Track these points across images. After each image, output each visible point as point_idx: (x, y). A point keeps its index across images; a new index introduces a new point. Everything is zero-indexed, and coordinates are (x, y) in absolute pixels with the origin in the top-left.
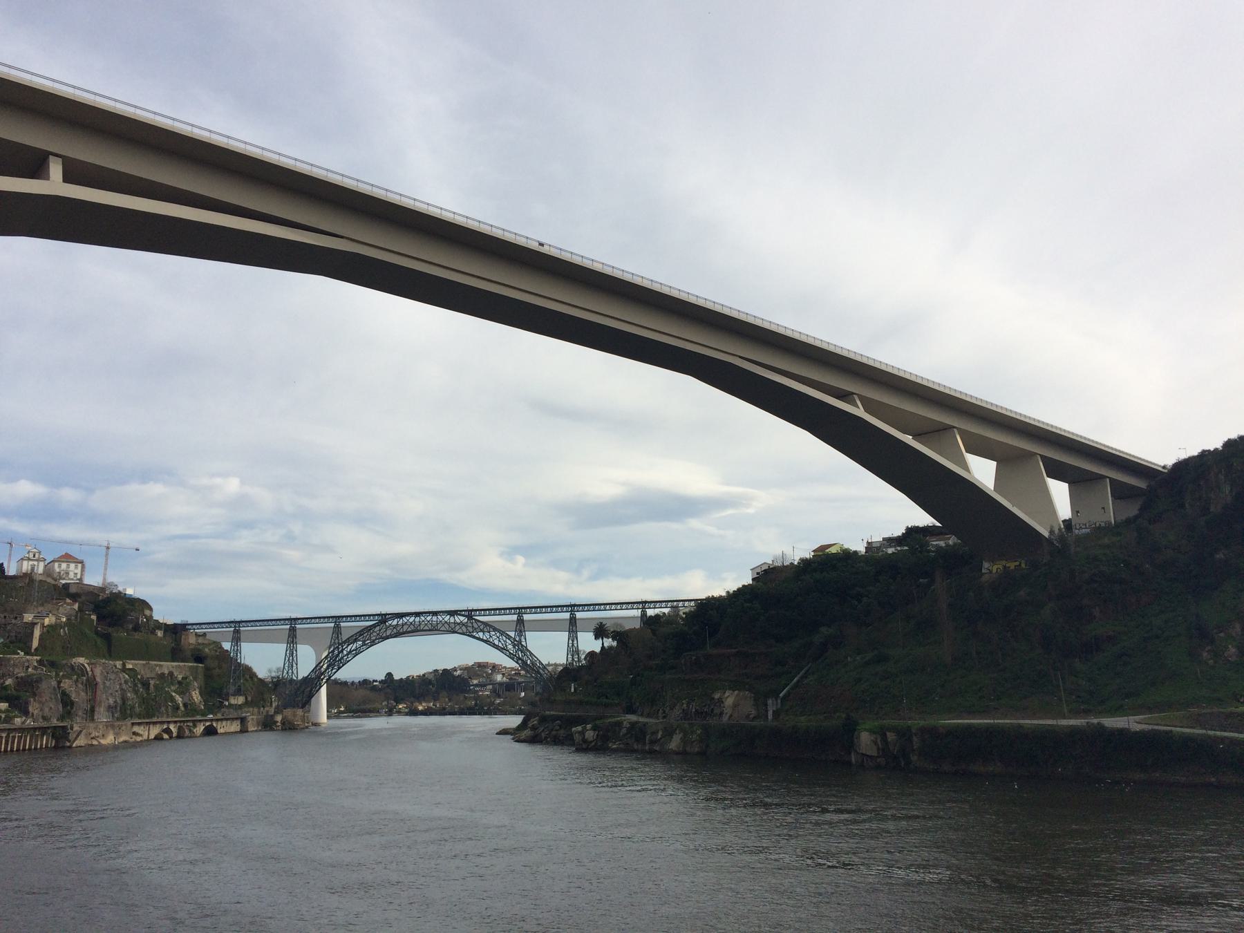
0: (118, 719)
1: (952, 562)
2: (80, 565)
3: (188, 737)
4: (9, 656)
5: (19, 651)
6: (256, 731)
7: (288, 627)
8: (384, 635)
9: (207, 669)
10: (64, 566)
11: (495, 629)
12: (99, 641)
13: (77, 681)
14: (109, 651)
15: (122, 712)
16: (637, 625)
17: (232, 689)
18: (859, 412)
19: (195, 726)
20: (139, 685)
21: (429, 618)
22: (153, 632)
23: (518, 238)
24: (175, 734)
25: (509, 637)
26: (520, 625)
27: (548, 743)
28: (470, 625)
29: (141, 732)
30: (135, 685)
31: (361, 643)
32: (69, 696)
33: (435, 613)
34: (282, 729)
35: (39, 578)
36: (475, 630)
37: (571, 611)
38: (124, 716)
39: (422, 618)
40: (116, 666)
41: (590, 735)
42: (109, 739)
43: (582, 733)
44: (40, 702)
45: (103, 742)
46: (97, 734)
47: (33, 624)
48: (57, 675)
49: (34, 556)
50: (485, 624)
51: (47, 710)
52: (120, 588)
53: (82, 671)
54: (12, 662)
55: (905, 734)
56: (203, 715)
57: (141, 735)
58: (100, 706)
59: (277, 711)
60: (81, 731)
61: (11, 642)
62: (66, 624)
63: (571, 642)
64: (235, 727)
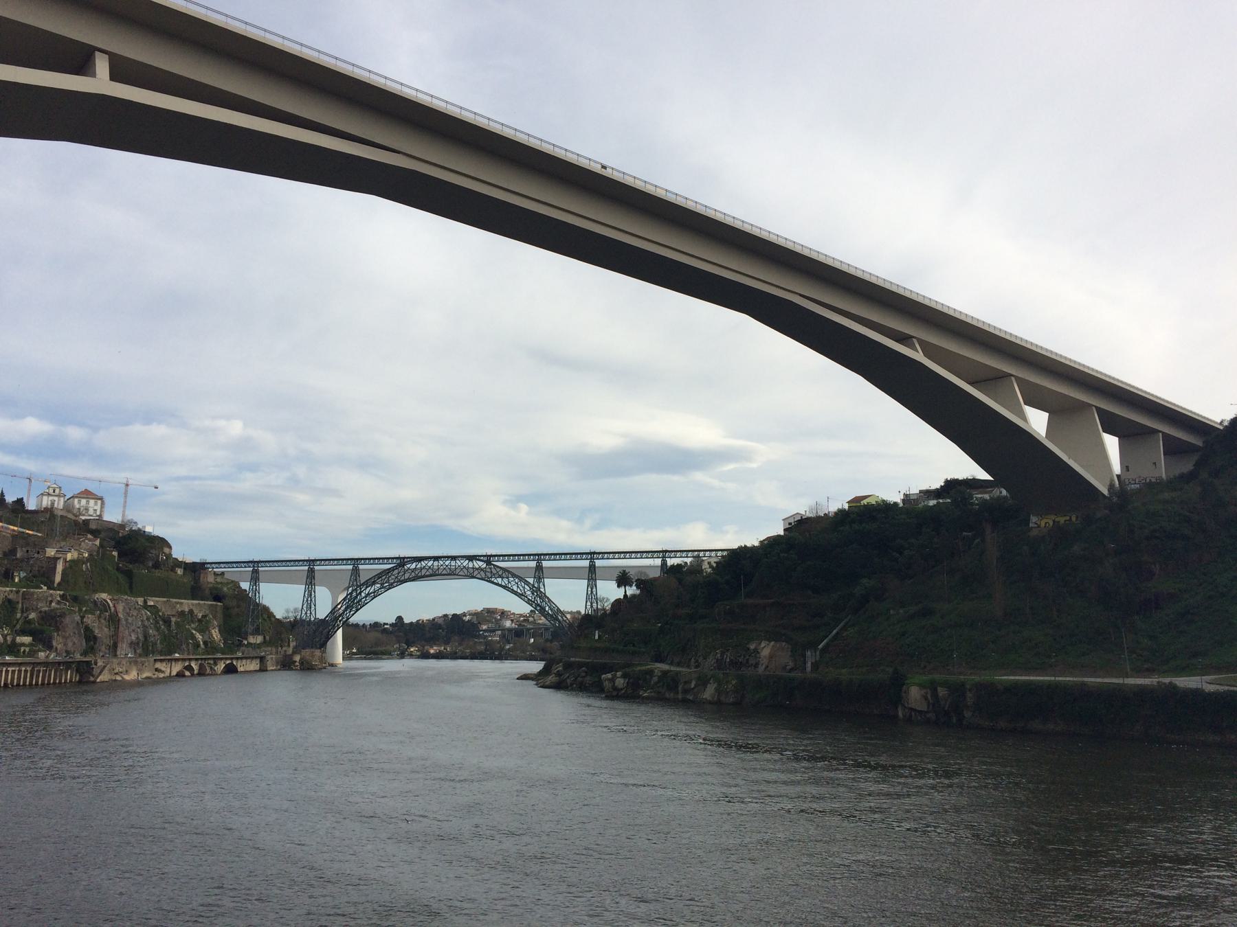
0: (140, 655)
1: (997, 514)
3: (208, 675)
4: (32, 590)
5: (42, 586)
7: (307, 568)
8: (403, 578)
9: (226, 608)
10: (84, 502)
11: (514, 576)
12: (120, 576)
13: (99, 617)
14: (131, 587)
15: (145, 648)
16: (657, 573)
17: (250, 628)
18: (918, 356)
19: (216, 664)
20: (161, 622)
21: (447, 563)
22: (173, 570)
23: (580, 159)
24: (196, 672)
25: (527, 583)
26: (539, 572)
27: (573, 690)
28: (489, 570)
29: (163, 669)
30: (157, 622)
31: (379, 585)
32: (92, 632)
33: (454, 558)
34: (301, 669)
35: (60, 513)
36: (493, 575)
37: (591, 559)
38: (146, 653)
39: (441, 562)
40: (137, 603)
41: (620, 682)
42: (132, 676)
43: (612, 680)
44: (64, 637)
45: (127, 677)
46: (121, 670)
47: (56, 559)
48: (80, 610)
49: (54, 491)
50: (504, 570)
51: (70, 644)
52: (140, 526)
53: (104, 607)
54: (35, 596)
55: (958, 690)
57: (163, 672)
58: (123, 642)
60: (105, 667)
62: (88, 560)
63: (589, 589)
64: (254, 665)
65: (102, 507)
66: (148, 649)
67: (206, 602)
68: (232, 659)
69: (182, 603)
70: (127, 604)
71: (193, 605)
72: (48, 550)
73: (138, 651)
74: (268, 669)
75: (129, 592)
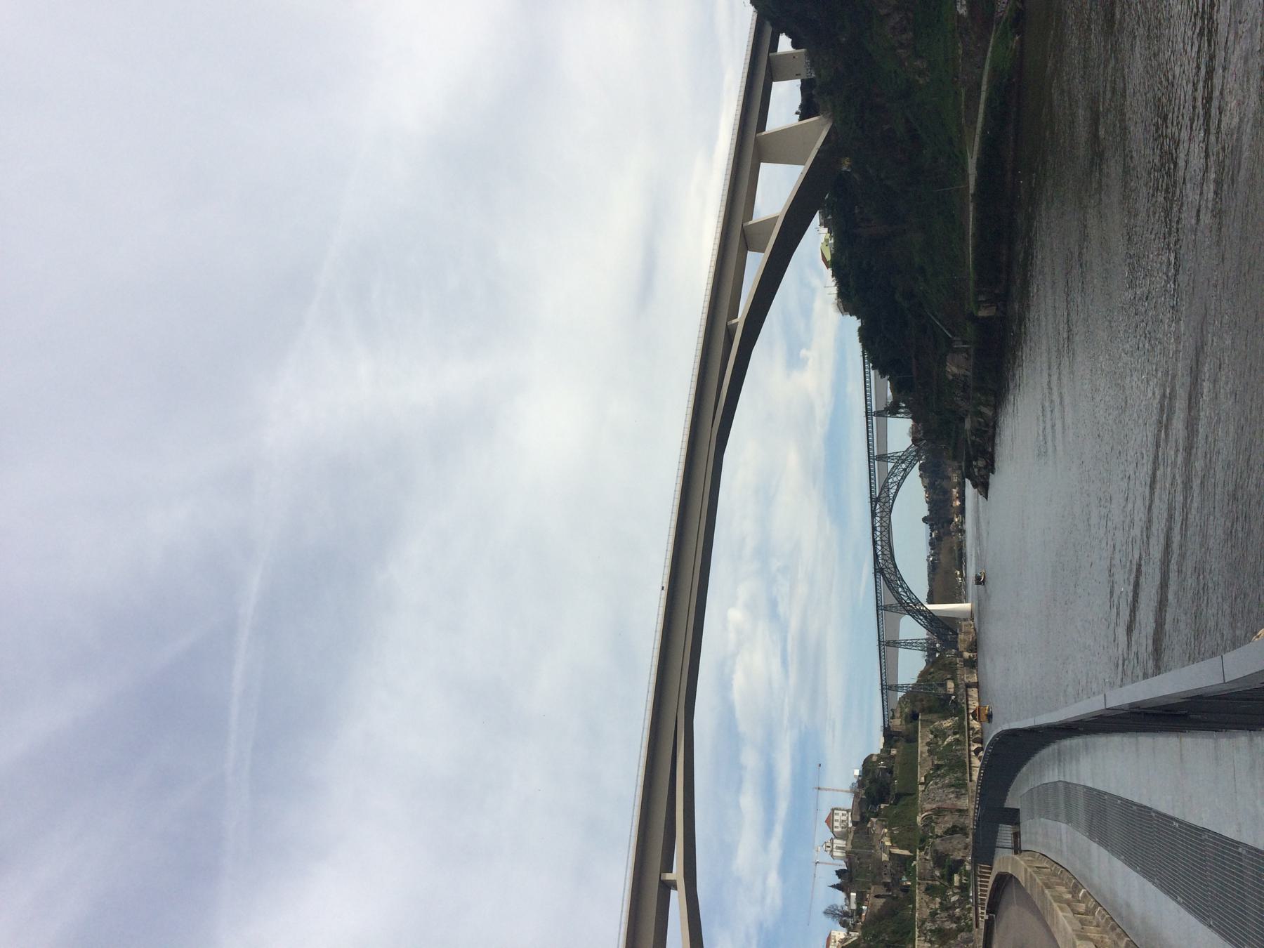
0: (967, 791)
2: (835, 811)
4: (917, 873)
6: (977, 674)
8: (893, 570)
9: (923, 711)
10: (836, 824)
12: (901, 803)
13: (936, 823)
14: (911, 795)
17: (941, 691)
19: (973, 729)
20: (939, 772)
22: (893, 757)
24: (980, 745)
30: (939, 776)
32: (949, 829)
35: (849, 847)
39: (878, 539)
40: (923, 791)
44: (953, 851)
47: (891, 854)
48: (931, 837)
49: (829, 847)
50: (882, 490)
51: (960, 846)
52: (855, 781)
53: (928, 820)
56: (964, 720)
58: (955, 805)
59: (960, 654)
61: (905, 870)
62: (889, 829)
63: (899, 416)
64: (974, 692)
65: (840, 810)
66: (962, 784)
67: (919, 731)
68: (968, 714)
69: (921, 752)
70: (925, 800)
71: (922, 743)
72: (883, 859)
73: (964, 792)
74: (976, 681)
75: (914, 796)
